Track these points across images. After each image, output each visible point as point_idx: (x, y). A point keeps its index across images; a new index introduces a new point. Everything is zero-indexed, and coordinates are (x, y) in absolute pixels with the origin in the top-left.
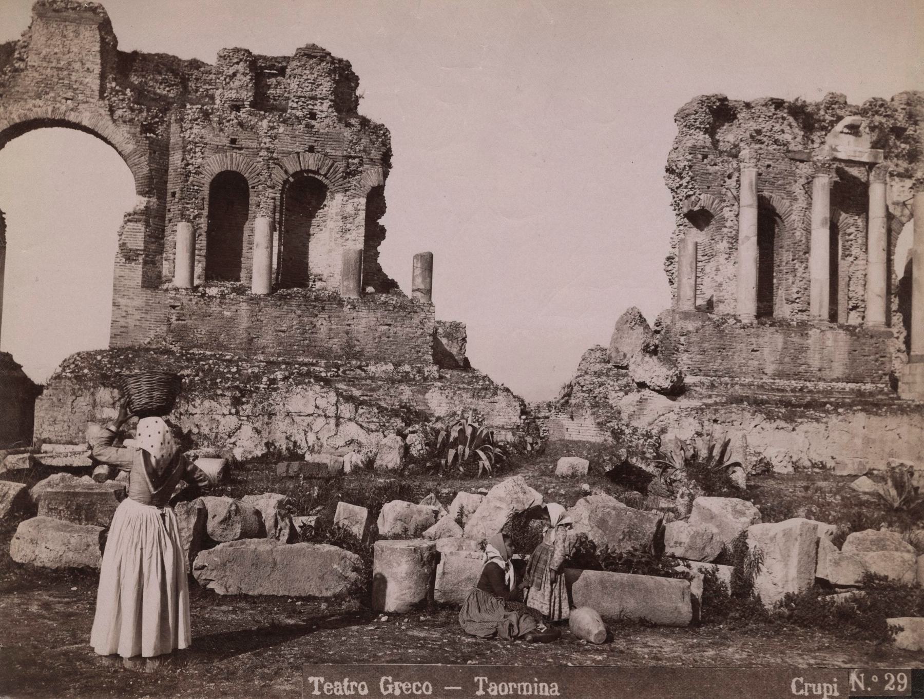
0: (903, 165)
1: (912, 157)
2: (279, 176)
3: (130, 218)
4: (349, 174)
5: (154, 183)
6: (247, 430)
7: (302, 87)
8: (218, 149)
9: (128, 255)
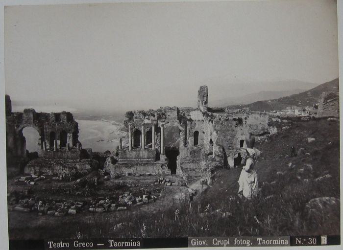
0: (164, 120)
1: (165, 118)
2: (59, 132)
3: (40, 139)
4: (69, 130)
5: (42, 134)
6: (51, 172)
7: (64, 118)
8: (51, 128)
9: (39, 144)
